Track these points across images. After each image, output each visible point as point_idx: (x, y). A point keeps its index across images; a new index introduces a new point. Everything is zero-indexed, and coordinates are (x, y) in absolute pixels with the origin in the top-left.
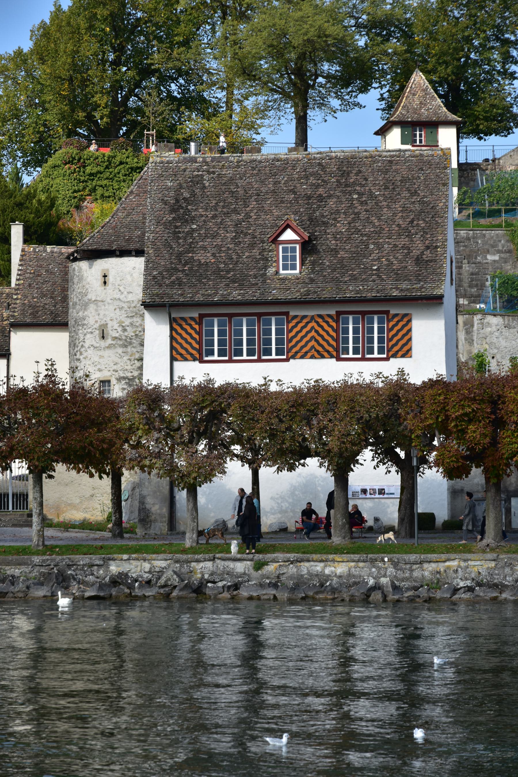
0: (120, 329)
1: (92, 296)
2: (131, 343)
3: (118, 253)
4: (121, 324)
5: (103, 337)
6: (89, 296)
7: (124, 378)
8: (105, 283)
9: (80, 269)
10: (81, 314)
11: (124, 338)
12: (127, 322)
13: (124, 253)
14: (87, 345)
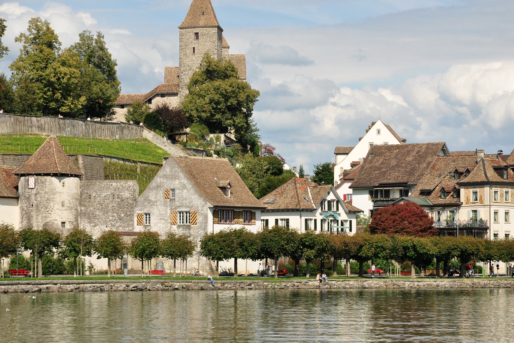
4: (69, 201)
9: (51, 180)
10: (51, 196)
13: (72, 176)
14: (55, 208)
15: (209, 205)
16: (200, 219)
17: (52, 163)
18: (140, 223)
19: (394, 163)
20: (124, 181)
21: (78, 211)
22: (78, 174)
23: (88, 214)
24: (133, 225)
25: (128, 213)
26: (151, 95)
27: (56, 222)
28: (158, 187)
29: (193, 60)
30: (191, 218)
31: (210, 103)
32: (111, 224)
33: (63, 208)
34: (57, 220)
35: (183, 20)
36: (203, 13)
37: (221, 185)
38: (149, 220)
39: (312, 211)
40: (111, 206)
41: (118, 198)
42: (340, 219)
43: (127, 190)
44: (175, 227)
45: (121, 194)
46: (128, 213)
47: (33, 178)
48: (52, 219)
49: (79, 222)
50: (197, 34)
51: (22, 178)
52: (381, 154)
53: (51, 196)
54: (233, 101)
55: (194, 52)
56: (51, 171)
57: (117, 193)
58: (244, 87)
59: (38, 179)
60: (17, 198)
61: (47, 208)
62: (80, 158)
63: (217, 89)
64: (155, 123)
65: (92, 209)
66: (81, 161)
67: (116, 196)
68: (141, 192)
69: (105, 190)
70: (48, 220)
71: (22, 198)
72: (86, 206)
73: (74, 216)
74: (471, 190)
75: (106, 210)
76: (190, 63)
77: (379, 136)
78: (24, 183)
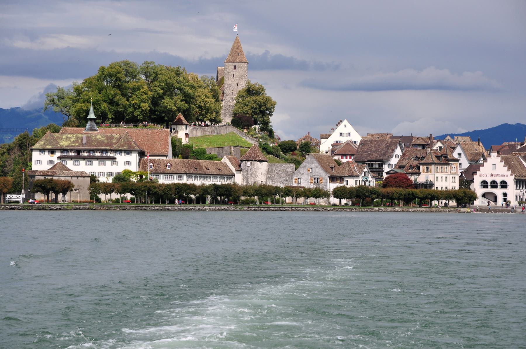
15: (328, 175)
16: (324, 181)
18: (296, 182)
19: (374, 149)
28: (304, 167)
29: (232, 81)
31: (252, 109)
39: (358, 176)
42: (369, 180)
44: (312, 184)
50: (235, 67)
51: (244, 162)
52: (366, 144)
54: (263, 108)
56: (257, 159)
58: (268, 100)
60: (241, 171)
62: (232, 148)
63: (255, 102)
64: (238, 124)
66: (232, 149)
68: (296, 169)
74: (425, 167)
77: (345, 128)
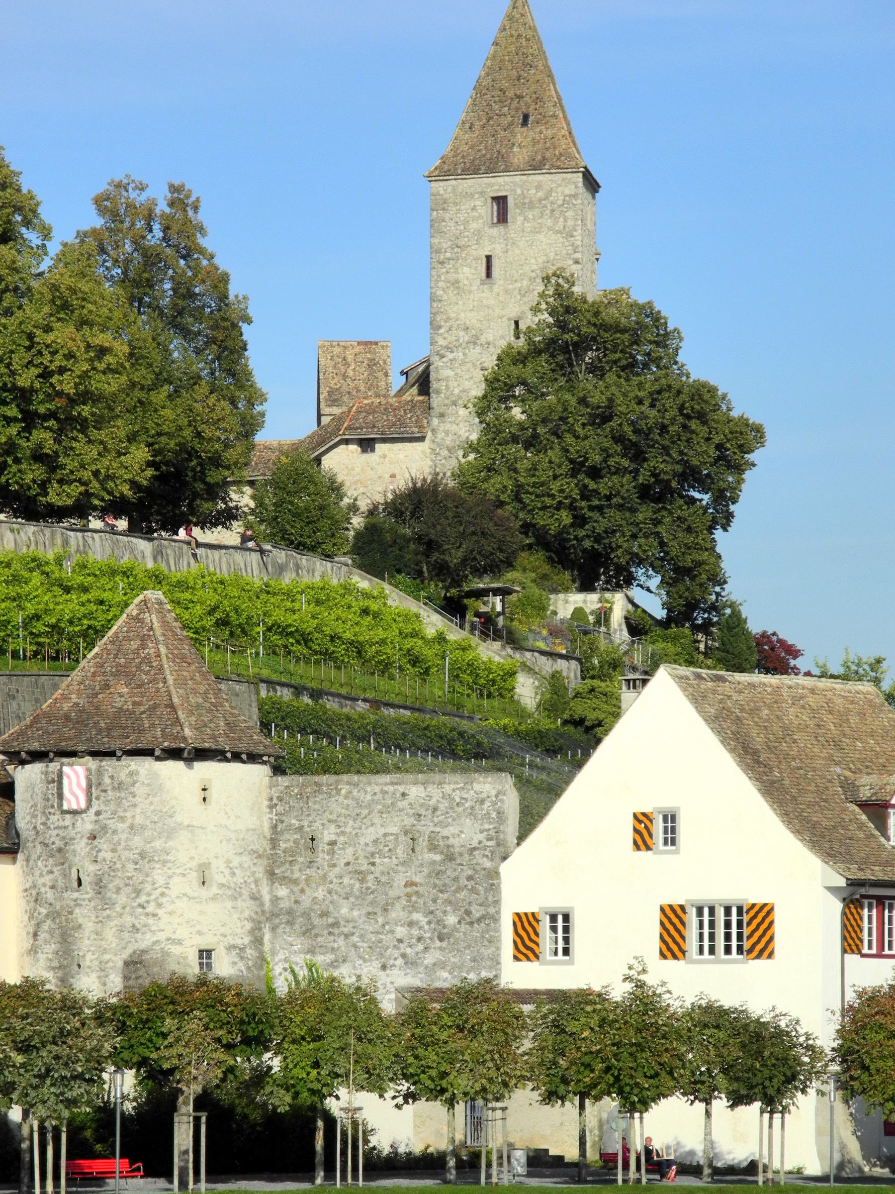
0: (227, 872)
1: (182, 818)
2: (241, 894)
3: (229, 755)
4: (228, 862)
5: (203, 883)
6: (178, 818)
7: (234, 947)
8: (204, 799)
9: (156, 775)
10: (158, 844)
11: (232, 885)
12: (235, 863)
13: (236, 757)
14: (173, 893)
17: (154, 707)
20: (457, 777)
21: (262, 904)
22: (260, 749)
23: (306, 915)
24: (496, 962)
25: (477, 912)
26: (320, 444)
27: (175, 950)
30: (746, 932)
32: (404, 956)
33: (204, 893)
34: (179, 942)
35: (445, 148)
36: (526, 118)
37: (865, 794)
38: (566, 940)
40: (400, 880)
41: (433, 848)
43: (472, 813)
45: (445, 832)
46: (477, 912)
47: (80, 770)
48: (161, 936)
49: (267, 947)
50: (501, 202)
53: (158, 844)
55: (489, 274)
57: (426, 827)
59: (100, 772)
61: (138, 892)
63: (602, 417)
65: (320, 893)
67: (423, 843)
69: (375, 814)
70: (145, 941)
71: (32, 848)
72: (295, 882)
73: (248, 926)
75: (382, 900)
76: (472, 319)
78: (40, 788)
